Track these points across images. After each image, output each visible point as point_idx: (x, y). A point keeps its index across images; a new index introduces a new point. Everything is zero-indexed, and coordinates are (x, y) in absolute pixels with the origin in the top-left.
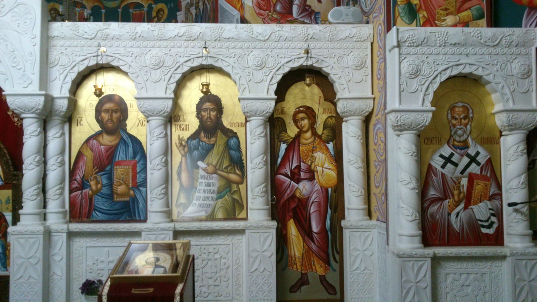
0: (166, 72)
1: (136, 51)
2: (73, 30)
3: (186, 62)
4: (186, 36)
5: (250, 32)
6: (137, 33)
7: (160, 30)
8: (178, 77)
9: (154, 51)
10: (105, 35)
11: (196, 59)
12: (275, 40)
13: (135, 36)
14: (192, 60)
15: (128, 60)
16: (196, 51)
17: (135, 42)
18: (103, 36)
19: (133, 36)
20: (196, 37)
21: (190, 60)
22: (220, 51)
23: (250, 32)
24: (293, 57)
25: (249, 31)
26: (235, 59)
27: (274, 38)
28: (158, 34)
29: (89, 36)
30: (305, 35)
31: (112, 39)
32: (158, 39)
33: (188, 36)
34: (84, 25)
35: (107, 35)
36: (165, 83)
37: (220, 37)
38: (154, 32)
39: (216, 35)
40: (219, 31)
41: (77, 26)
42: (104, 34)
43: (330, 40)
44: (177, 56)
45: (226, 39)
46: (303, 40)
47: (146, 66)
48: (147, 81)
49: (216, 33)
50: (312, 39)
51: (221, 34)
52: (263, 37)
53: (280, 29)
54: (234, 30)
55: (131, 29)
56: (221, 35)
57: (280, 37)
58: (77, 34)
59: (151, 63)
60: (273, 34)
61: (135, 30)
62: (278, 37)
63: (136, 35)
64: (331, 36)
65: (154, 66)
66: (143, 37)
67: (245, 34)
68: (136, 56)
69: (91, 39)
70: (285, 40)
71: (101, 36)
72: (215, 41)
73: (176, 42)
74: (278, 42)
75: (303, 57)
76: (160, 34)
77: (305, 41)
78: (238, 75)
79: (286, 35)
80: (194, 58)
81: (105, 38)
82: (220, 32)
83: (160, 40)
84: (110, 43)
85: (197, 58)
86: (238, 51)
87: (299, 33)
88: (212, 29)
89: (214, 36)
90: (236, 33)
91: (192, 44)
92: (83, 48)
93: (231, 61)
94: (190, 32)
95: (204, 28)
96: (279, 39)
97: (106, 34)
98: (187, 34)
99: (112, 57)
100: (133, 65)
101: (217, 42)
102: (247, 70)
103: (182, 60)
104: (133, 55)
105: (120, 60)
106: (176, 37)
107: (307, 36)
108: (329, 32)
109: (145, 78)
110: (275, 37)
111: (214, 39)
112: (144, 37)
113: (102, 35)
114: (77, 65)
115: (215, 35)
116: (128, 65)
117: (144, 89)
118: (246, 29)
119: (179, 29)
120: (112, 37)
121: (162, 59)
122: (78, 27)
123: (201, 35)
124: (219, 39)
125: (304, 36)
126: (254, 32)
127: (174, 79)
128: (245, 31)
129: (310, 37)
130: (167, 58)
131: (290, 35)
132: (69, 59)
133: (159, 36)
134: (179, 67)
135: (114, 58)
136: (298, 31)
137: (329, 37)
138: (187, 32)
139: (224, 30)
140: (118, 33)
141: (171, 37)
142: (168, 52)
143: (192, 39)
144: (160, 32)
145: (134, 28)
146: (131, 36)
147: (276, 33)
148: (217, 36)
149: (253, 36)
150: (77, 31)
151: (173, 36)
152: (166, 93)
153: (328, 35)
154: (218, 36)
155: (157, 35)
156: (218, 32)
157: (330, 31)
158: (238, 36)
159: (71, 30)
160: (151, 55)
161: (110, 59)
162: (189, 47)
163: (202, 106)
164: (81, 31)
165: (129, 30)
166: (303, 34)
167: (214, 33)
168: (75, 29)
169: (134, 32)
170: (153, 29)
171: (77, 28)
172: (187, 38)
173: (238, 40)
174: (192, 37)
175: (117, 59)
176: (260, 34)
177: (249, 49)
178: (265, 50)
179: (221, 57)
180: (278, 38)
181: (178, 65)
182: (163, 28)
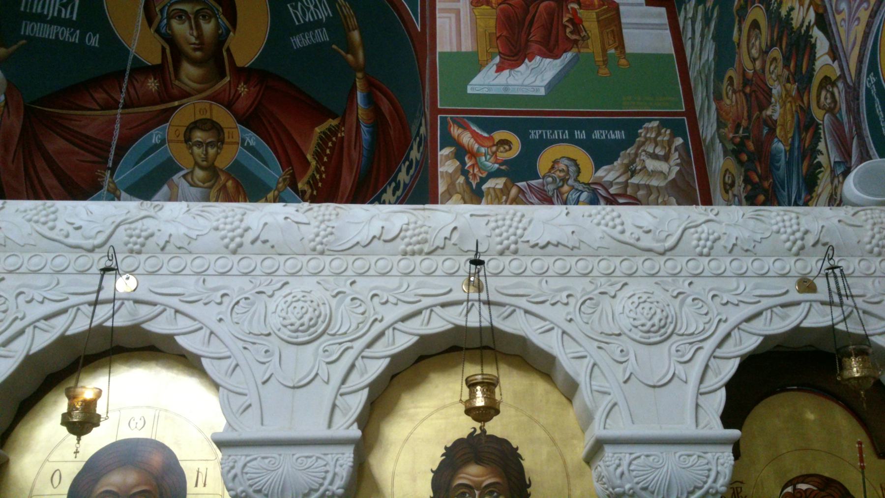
0: (337, 351)
1: (237, 286)
2: (37, 222)
3: (404, 319)
4: (407, 240)
5: (614, 227)
6: (247, 229)
7: (322, 222)
8: (375, 368)
9: (297, 286)
10: (139, 237)
11: (438, 309)
12: (698, 250)
13: (238, 240)
14: (426, 313)
15: (208, 314)
16: (438, 285)
17: (236, 258)
18: (134, 239)
19: (232, 240)
20: (439, 242)
21: (418, 313)
22: (517, 286)
23: (614, 227)
24: (765, 303)
25: (611, 224)
26: (570, 308)
27: (694, 243)
28: (317, 235)
29: (86, 238)
30: (793, 233)
31: (163, 249)
32: (314, 250)
33: (414, 239)
34: (74, 207)
35: (147, 238)
36: (329, 392)
37: (516, 243)
38: (302, 227)
39: (505, 235)
40: (515, 224)
41: (53, 209)
42: (137, 232)
43: (876, 250)
44: (376, 299)
45: (537, 249)
46: (790, 250)
47: (269, 335)
48: (264, 383)
49: (504, 228)
50: (819, 246)
51: (519, 232)
52: (658, 241)
53: (711, 216)
54: (563, 218)
55: (229, 220)
56: (521, 237)
57: (715, 241)
58: (45, 230)
59: (287, 322)
60: (692, 230)
61: (241, 221)
62: (707, 240)
63: (242, 236)
64: (877, 236)
65: (296, 331)
66: (265, 242)
67: (598, 232)
68: (237, 303)
69: (92, 250)
70: (731, 251)
71: (127, 239)
72: (502, 253)
73: (373, 259)
74: (708, 255)
75: (798, 303)
76: (322, 233)
77: (797, 254)
78: (586, 361)
79: (735, 235)
80: (431, 308)
81: (137, 247)
82: (517, 228)
83: (322, 253)
84: (152, 261)
85: (443, 305)
86: (580, 286)
87: (775, 228)
88: (493, 219)
89: (498, 239)
90: (570, 230)
91: (426, 263)
92: (61, 277)
93: (558, 315)
94: (422, 226)
95: (468, 216)
96: (711, 248)
97: (144, 234)
98: (409, 233)
99: (154, 304)
100: (222, 330)
101: (506, 259)
102: (615, 348)
103: (392, 314)
104: (226, 299)
105: (179, 316)
106: (376, 240)
107: (802, 239)
108: (869, 227)
109: (261, 373)
110: (699, 239)
111: (499, 247)
112: (268, 245)
113: (131, 236)
114: (29, 331)
115: (501, 235)
116: (205, 332)
117: (254, 411)
118: (599, 217)
119: (386, 220)
120: (162, 244)
121: (325, 310)
122: (54, 213)
123: (456, 236)
124: (513, 247)
125: (792, 238)
126: (625, 226)
127: (362, 375)
128: (599, 224)
129: (810, 239)
130: (342, 307)
131: (747, 234)
132: (5, 312)
133: (318, 239)
134: (382, 334)
135: (159, 308)
136: (772, 225)
137: (874, 242)
138: (412, 226)
139: (530, 222)
140: (183, 230)
141: (358, 243)
142: (347, 289)
143: (426, 248)
144: (323, 226)
145: (239, 217)
146: (227, 241)
147: (699, 229)
148: (508, 239)
149: (626, 237)
150: (51, 224)
151: (364, 238)
152: (330, 426)
153: (870, 233)
154: (513, 238)
155: (312, 236)
156: (510, 226)
157: (871, 221)
158: (575, 237)
159: (29, 220)
160: (289, 298)
161: (144, 311)
162: (416, 273)
163: (452, 477)
164: (60, 224)
165: (222, 220)
166: (789, 230)
167: (497, 231)
168: (43, 219)
169: (239, 227)
170: (301, 218)
171: (52, 216)
172: (410, 244)
173: (576, 251)
174: (425, 241)
175: (170, 312)
176: (649, 232)
177: (613, 280)
178: (670, 279)
179: (523, 302)
180: (709, 243)
181: (377, 328)
182: (333, 217)
